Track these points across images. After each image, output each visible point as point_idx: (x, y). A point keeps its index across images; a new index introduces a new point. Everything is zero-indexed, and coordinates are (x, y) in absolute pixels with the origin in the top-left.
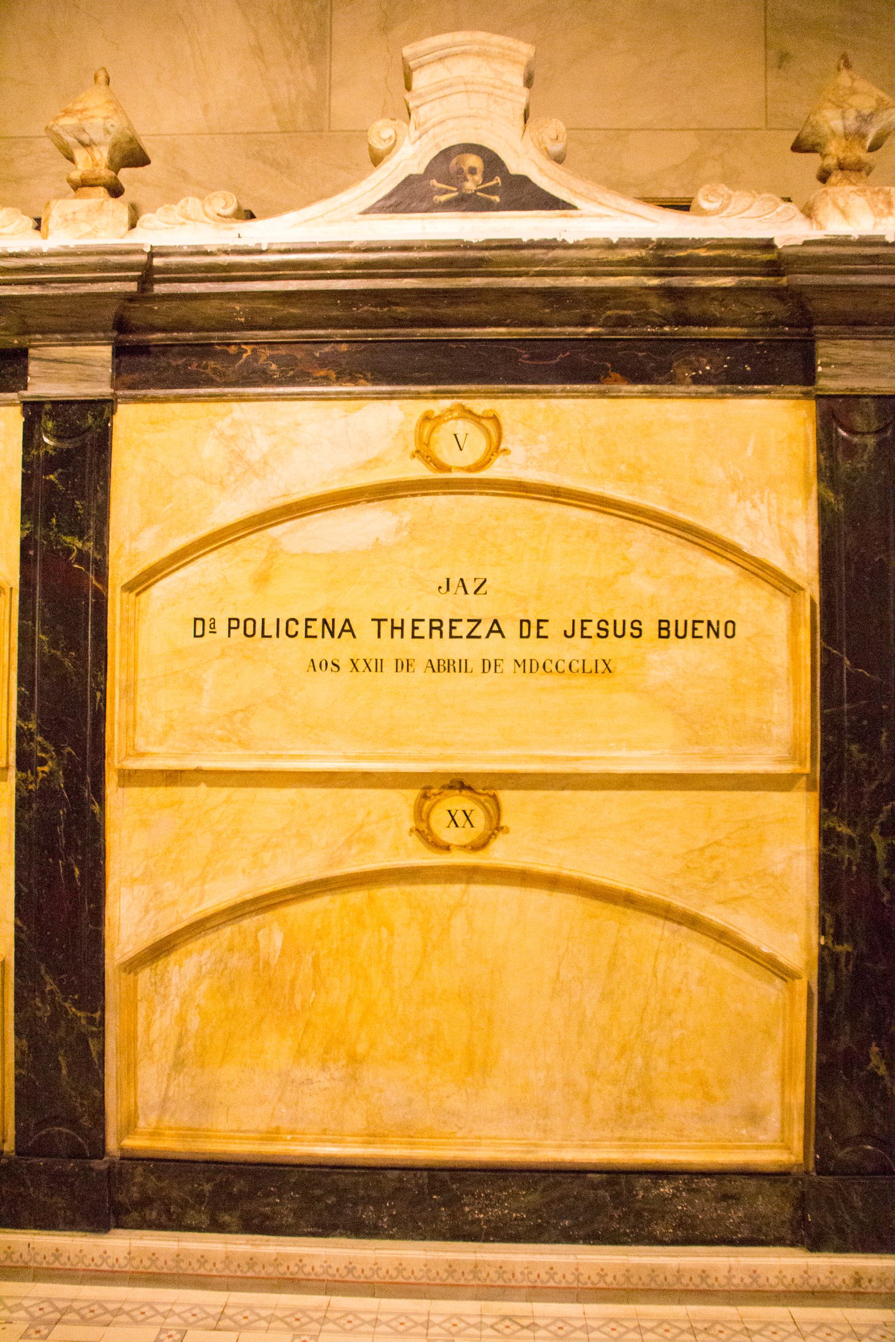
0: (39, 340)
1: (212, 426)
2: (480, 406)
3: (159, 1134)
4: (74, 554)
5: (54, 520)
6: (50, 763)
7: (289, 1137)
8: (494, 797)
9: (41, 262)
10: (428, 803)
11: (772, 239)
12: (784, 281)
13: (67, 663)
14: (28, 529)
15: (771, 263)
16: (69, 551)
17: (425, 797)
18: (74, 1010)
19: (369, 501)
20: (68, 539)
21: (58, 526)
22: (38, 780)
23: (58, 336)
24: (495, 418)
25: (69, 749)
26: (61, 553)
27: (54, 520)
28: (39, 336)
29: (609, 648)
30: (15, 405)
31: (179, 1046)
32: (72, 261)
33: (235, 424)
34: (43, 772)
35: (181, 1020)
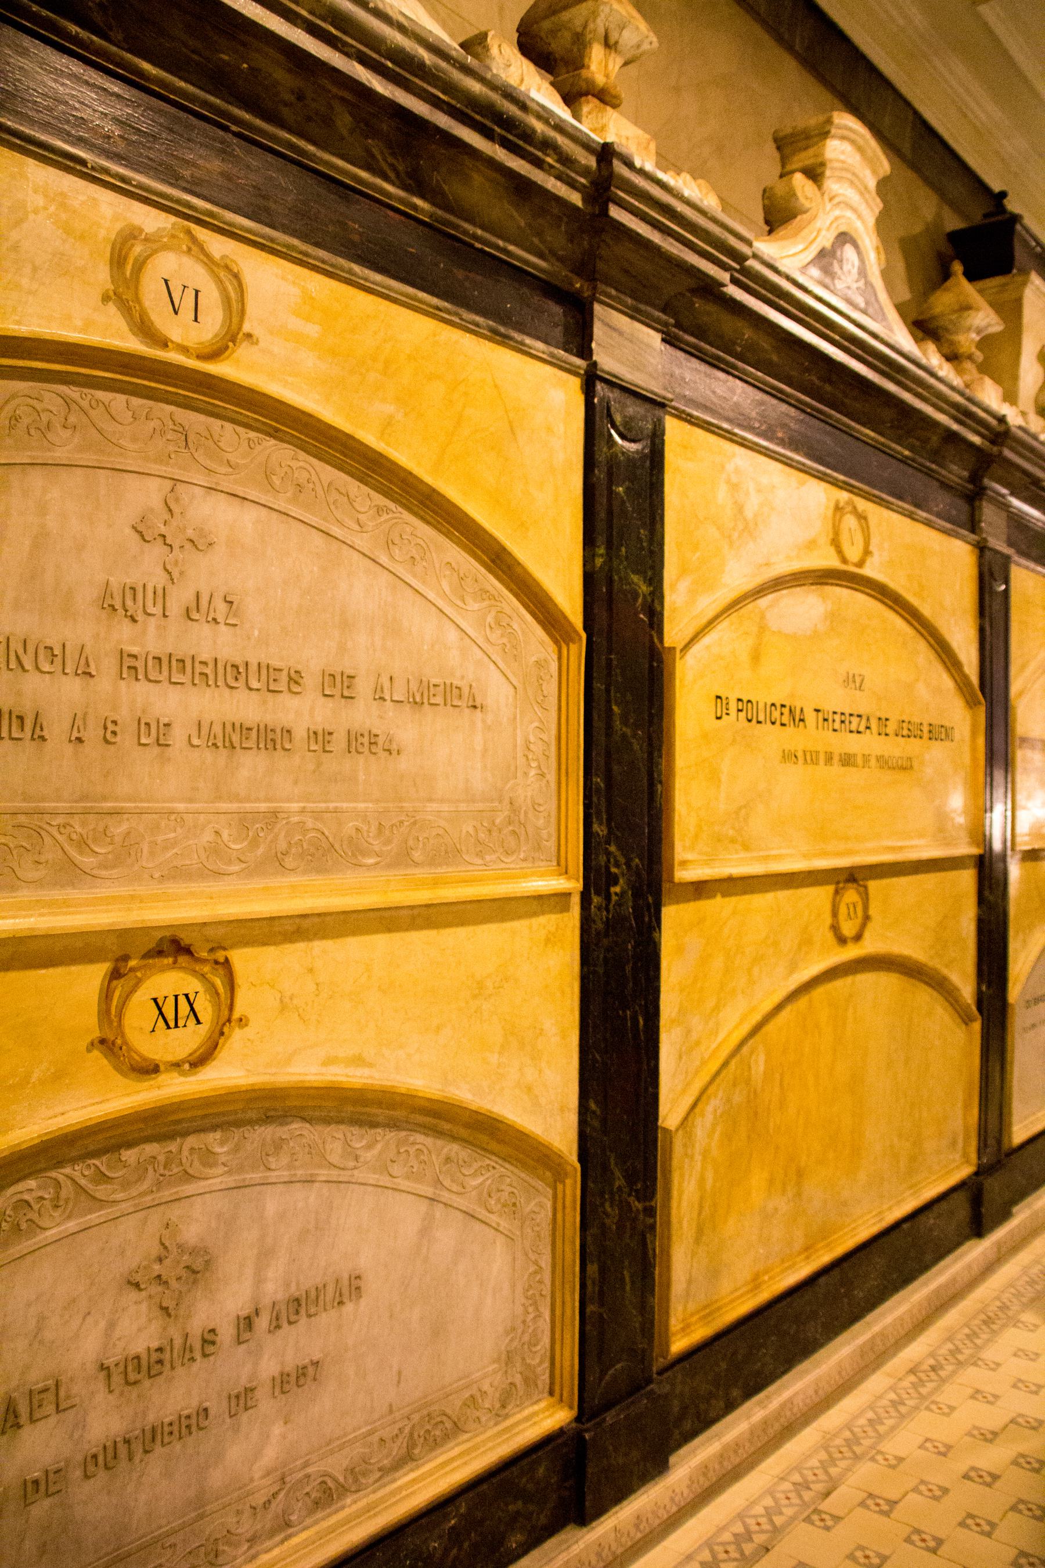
0: (609, 296)
1: (723, 467)
2: (862, 504)
3: (688, 1326)
4: (640, 600)
5: (623, 549)
6: (621, 881)
7: (766, 1278)
8: (866, 887)
9: (680, 207)
10: (838, 898)
11: (1004, 416)
12: (995, 449)
13: (636, 747)
14: (602, 555)
15: (998, 435)
16: (635, 595)
17: (837, 892)
18: (636, 1203)
19: (812, 584)
20: (635, 578)
21: (627, 558)
22: (611, 906)
23: (629, 301)
24: (865, 518)
25: (637, 860)
26: (629, 596)
27: (623, 549)
28: (613, 292)
29: (913, 746)
30: (576, 374)
31: (700, 1214)
32: (702, 221)
33: (737, 471)
34: (616, 894)
35: (702, 1180)
